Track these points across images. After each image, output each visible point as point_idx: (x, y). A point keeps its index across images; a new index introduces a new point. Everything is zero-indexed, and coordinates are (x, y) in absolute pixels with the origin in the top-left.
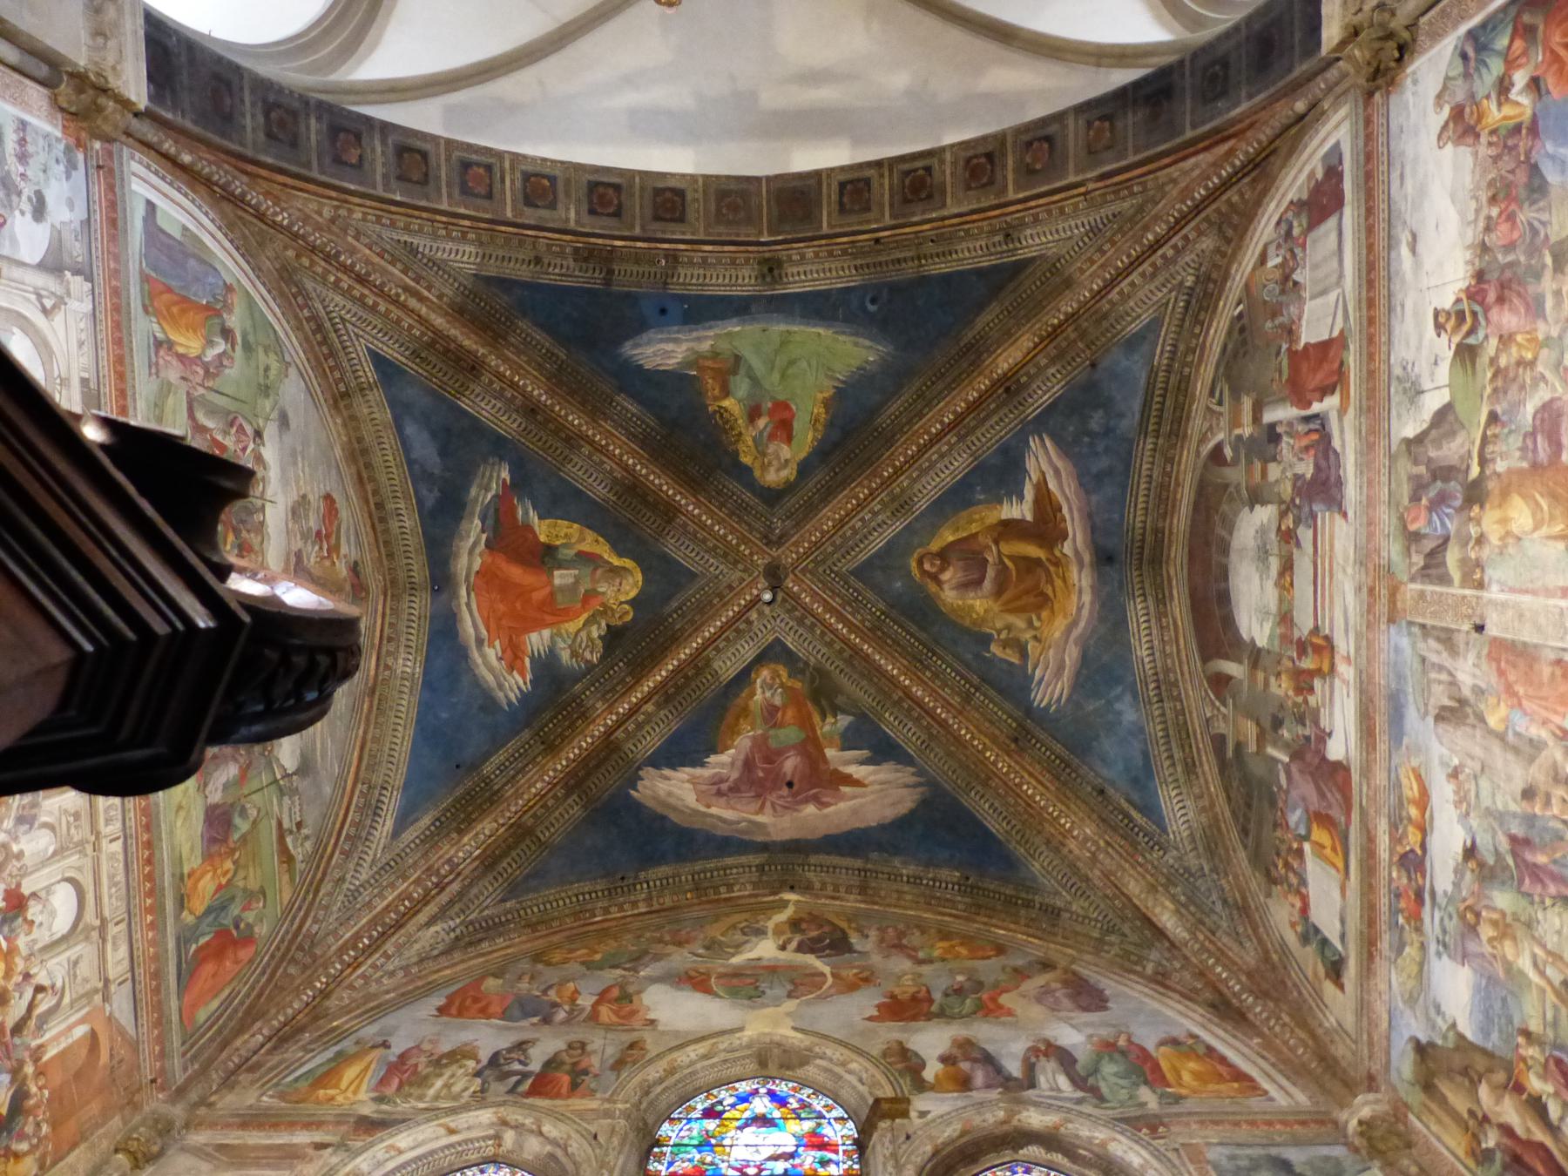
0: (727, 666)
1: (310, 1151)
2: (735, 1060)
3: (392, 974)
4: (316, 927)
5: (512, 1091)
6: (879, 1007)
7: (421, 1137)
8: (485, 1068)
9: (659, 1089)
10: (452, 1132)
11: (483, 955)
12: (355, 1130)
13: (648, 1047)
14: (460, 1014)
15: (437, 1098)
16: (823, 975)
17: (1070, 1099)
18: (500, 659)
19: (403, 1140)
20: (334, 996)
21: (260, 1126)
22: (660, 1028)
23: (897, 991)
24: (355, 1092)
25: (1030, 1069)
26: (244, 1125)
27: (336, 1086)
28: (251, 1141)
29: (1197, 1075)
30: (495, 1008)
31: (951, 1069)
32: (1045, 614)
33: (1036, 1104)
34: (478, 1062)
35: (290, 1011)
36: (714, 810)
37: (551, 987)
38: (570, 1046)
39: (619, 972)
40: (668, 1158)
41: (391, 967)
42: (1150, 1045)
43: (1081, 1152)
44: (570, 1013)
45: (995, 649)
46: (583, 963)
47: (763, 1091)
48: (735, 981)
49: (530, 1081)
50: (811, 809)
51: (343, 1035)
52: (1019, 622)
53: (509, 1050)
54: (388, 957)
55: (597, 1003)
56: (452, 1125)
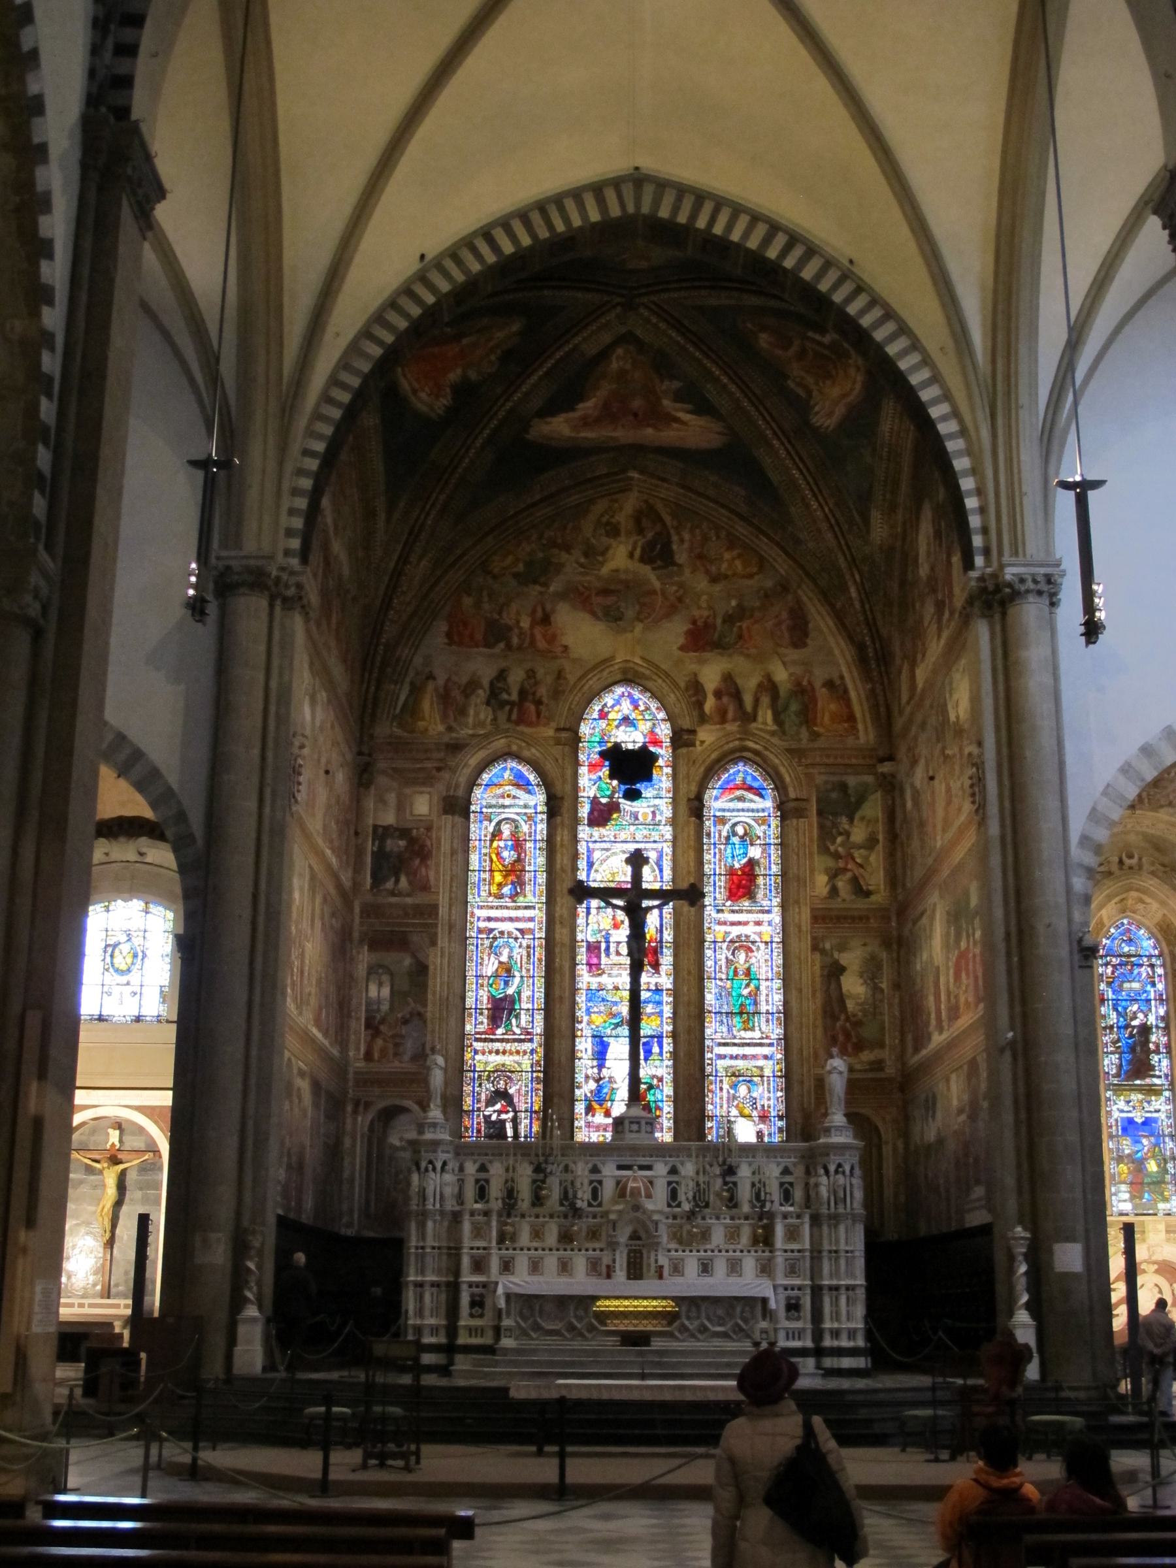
0: (591, 349)
1: (434, 772)
5: (509, 720)
6: (690, 633)
13: (568, 676)
15: (474, 727)
16: (654, 592)
18: (429, 395)
23: (696, 613)
25: (757, 701)
27: (423, 719)
32: (828, 382)
36: (583, 435)
38: (529, 677)
39: (538, 588)
42: (818, 684)
45: (791, 384)
49: (515, 711)
50: (650, 431)
52: (810, 380)
55: (532, 627)
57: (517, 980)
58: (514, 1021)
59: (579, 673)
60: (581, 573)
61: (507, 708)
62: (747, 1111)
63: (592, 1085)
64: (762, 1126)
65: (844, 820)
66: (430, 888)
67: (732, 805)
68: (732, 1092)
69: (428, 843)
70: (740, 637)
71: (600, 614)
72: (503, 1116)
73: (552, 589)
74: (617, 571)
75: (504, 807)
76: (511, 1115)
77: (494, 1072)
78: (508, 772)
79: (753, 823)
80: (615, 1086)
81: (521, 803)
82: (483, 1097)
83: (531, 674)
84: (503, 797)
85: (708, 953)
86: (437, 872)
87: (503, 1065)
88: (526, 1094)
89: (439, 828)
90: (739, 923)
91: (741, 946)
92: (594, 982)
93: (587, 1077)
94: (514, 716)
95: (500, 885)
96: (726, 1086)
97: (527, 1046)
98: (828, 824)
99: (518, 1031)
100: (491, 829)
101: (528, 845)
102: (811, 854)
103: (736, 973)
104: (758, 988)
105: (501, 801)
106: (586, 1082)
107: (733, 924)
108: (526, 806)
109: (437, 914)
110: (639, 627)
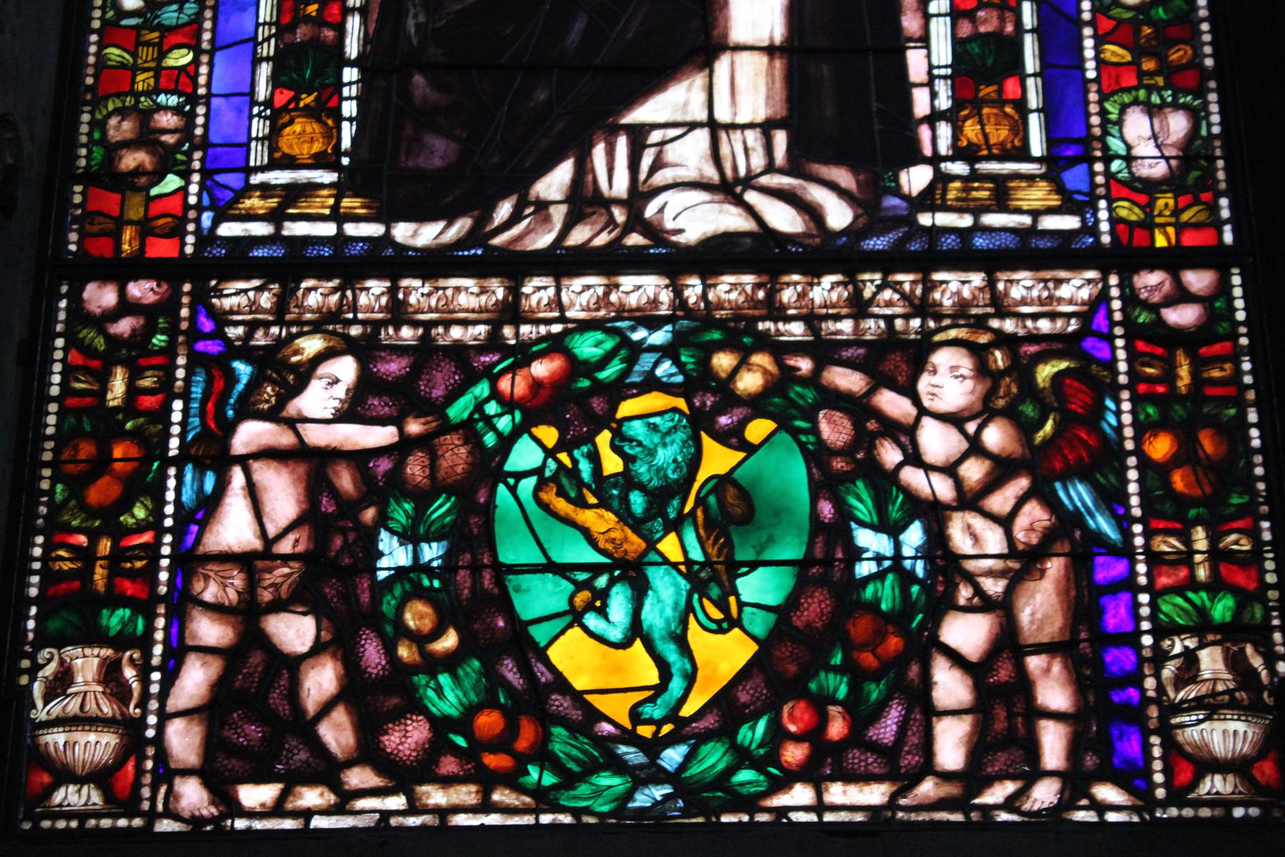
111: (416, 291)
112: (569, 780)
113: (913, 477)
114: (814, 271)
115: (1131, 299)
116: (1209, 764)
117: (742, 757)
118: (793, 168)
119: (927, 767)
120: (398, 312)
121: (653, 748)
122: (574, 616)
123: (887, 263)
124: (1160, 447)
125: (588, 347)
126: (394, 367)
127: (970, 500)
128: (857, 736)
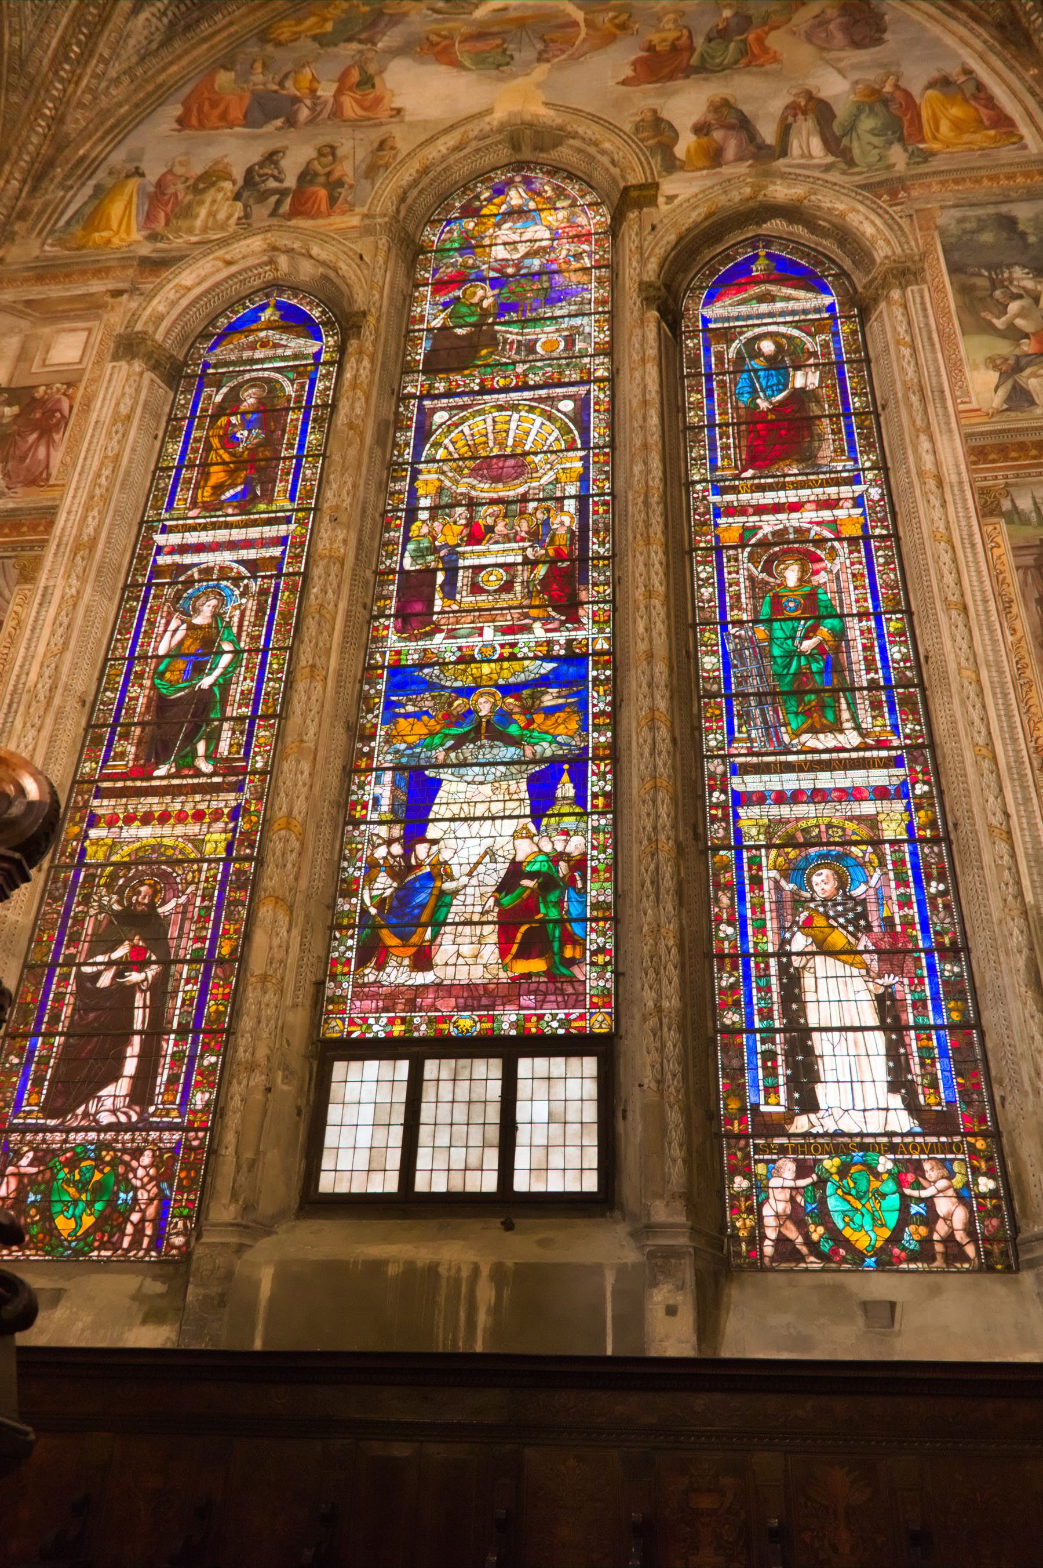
1: (108, 299)
2: (487, 148)
3: (116, 81)
4: (16, 40)
5: (274, 213)
7: (203, 273)
8: (243, 188)
9: (415, 192)
10: (229, 263)
11: (205, 40)
12: (142, 273)
13: (399, 144)
14: (202, 126)
15: (205, 229)
16: (575, 24)
17: (818, 166)
19: (187, 278)
20: (69, 119)
21: (55, 278)
22: (407, 118)
23: (655, 38)
24: (128, 231)
25: (785, 131)
26: (40, 279)
27: (108, 228)
28: (54, 295)
29: (958, 126)
30: (236, 113)
31: (704, 140)
33: (783, 176)
34: (234, 183)
35: (31, 148)
37: (286, 76)
38: (321, 154)
39: (355, 46)
40: (433, 265)
41: (113, 73)
42: (916, 89)
43: (821, 223)
44: (312, 109)
46: (315, 38)
47: (518, 179)
48: (481, 45)
49: (289, 200)
51: (95, 165)
53: (262, 164)
54: (106, 62)
55: (339, 93)
56: (228, 257)
57: (225, 660)
58: (201, 747)
59: (423, 137)
60: (436, 21)
61: (274, 199)
62: (839, 939)
63: (384, 884)
64: (888, 980)
65: (1018, 272)
66: (48, 480)
67: (744, 309)
68: (788, 887)
69: (65, 404)
70: (744, 51)
71: (467, 63)
72: (134, 977)
73: (380, 45)
74: (505, 9)
75: (252, 361)
76: (151, 972)
77: (127, 865)
78: (269, 311)
79: (796, 333)
80: (448, 886)
81: (288, 352)
82: (89, 926)
83: (329, 151)
84: (253, 347)
85: (704, 572)
86: (72, 450)
87: (154, 848)
88: (204, 918)
89: (93, 381)
90: (776, 508)
91: (784, 552)
92: (411, 651)
93: (372, 866)
94: (286, 207)
95: (219, 488)
96: (768, 874)
97: (227, 801)
98: (982, 282)
99: (206, 767)
100: (218, 398)
101: (291, 416)
102: (947, 339)
103: (777, 604)
104: (840, 635)
105: (247, 354)
106: (370, 880)
107: (761, 510)
108: (296, 357)
109: (51, 524)
110: (546, 66)
111: (48, 1136)
112: (53, 1249)
113: (134, 1181)
114: (126, 1132)
115: (187, 1139)
116: (174, 1247)
117: (87, 1244)
118: (129, 1107)
119: (120, 1248)
120: (44, 1141)
121: (70, 1242)
122: (62, 1212)
123: (140, 1130)
124: (183, 1175)
125: (79, 1150)
126: (40, 1154)
127: (143, 1187)
128: (109, 1241)
